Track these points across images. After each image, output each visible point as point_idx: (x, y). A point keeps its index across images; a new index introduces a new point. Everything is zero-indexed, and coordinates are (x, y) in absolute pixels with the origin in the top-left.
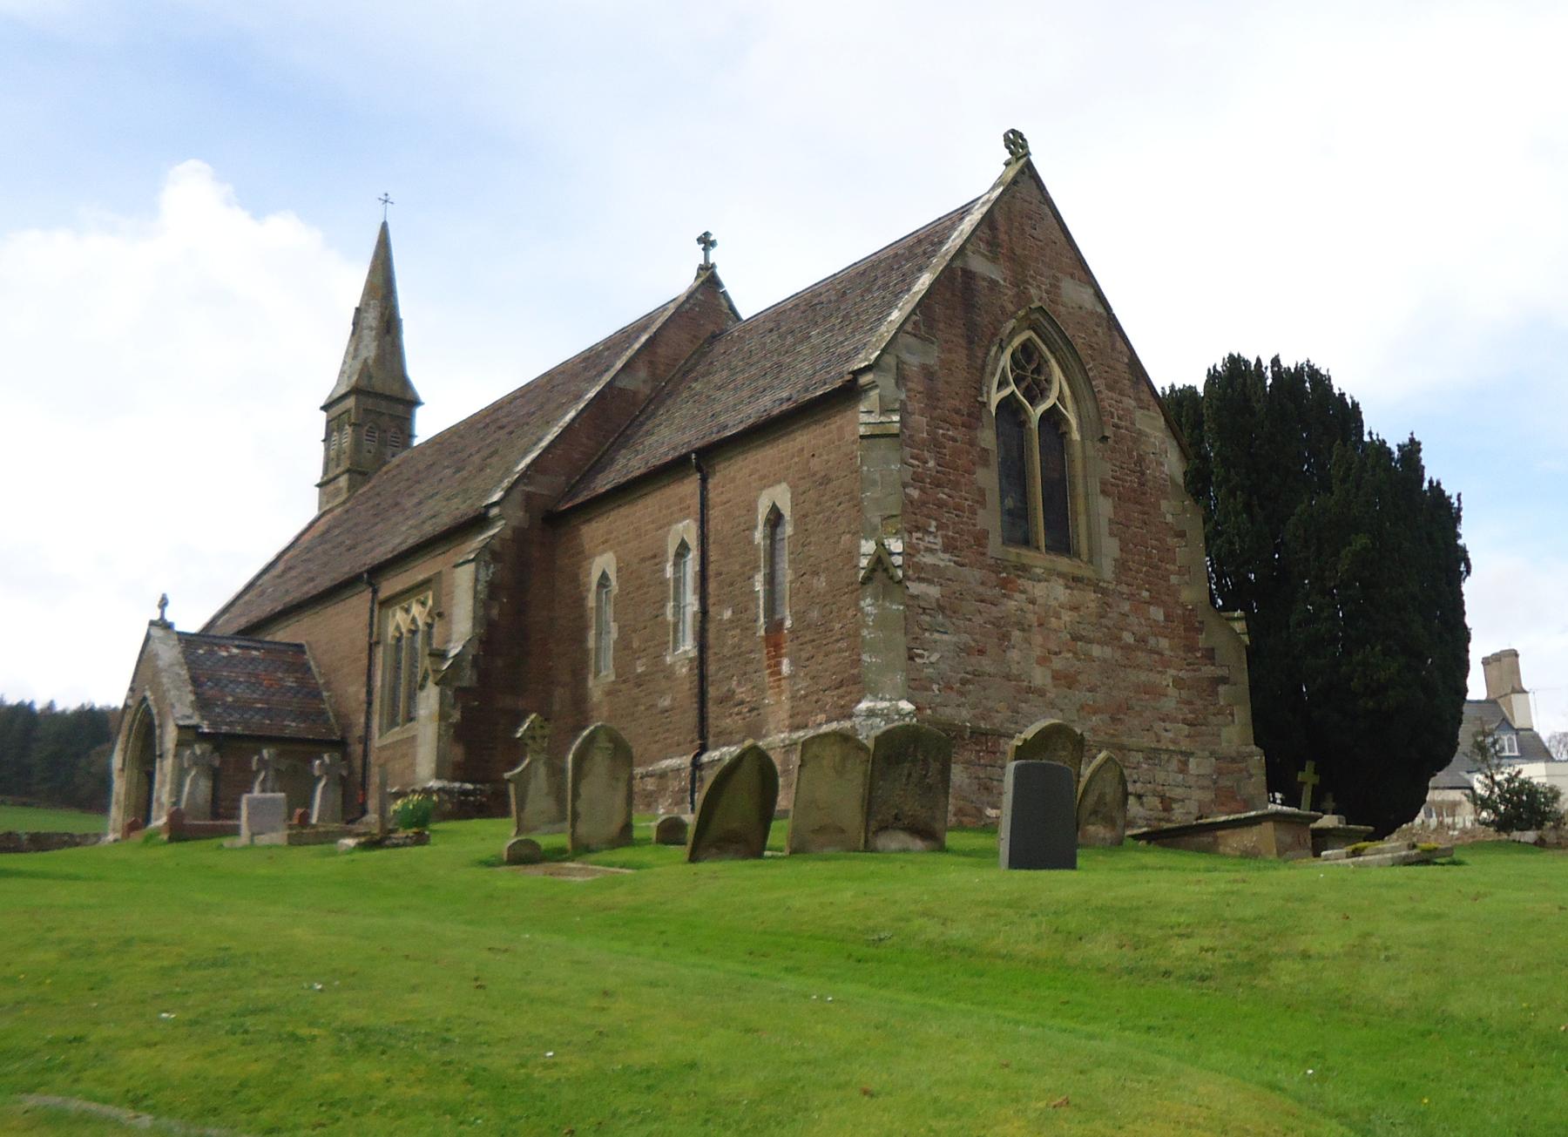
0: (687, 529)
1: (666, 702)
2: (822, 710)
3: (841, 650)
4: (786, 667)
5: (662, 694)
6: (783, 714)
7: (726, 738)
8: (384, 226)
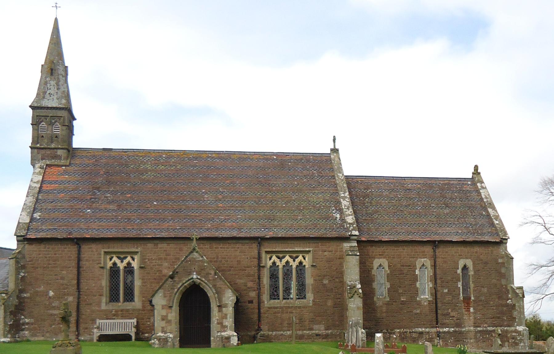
0: (428, 263)
1: (418, 311)
2: (486, 323)
3: (493, 309)
4: (472, 310)
5: (415, 309)
6: (471, 322)
7: (444, 325)
8: (56, 20)
